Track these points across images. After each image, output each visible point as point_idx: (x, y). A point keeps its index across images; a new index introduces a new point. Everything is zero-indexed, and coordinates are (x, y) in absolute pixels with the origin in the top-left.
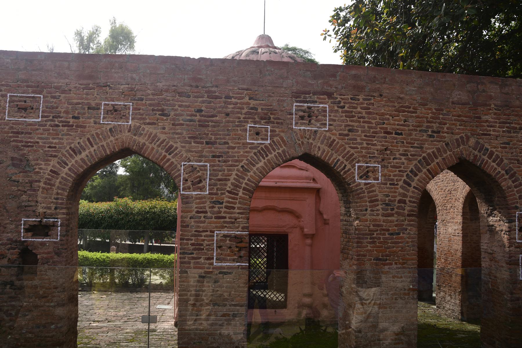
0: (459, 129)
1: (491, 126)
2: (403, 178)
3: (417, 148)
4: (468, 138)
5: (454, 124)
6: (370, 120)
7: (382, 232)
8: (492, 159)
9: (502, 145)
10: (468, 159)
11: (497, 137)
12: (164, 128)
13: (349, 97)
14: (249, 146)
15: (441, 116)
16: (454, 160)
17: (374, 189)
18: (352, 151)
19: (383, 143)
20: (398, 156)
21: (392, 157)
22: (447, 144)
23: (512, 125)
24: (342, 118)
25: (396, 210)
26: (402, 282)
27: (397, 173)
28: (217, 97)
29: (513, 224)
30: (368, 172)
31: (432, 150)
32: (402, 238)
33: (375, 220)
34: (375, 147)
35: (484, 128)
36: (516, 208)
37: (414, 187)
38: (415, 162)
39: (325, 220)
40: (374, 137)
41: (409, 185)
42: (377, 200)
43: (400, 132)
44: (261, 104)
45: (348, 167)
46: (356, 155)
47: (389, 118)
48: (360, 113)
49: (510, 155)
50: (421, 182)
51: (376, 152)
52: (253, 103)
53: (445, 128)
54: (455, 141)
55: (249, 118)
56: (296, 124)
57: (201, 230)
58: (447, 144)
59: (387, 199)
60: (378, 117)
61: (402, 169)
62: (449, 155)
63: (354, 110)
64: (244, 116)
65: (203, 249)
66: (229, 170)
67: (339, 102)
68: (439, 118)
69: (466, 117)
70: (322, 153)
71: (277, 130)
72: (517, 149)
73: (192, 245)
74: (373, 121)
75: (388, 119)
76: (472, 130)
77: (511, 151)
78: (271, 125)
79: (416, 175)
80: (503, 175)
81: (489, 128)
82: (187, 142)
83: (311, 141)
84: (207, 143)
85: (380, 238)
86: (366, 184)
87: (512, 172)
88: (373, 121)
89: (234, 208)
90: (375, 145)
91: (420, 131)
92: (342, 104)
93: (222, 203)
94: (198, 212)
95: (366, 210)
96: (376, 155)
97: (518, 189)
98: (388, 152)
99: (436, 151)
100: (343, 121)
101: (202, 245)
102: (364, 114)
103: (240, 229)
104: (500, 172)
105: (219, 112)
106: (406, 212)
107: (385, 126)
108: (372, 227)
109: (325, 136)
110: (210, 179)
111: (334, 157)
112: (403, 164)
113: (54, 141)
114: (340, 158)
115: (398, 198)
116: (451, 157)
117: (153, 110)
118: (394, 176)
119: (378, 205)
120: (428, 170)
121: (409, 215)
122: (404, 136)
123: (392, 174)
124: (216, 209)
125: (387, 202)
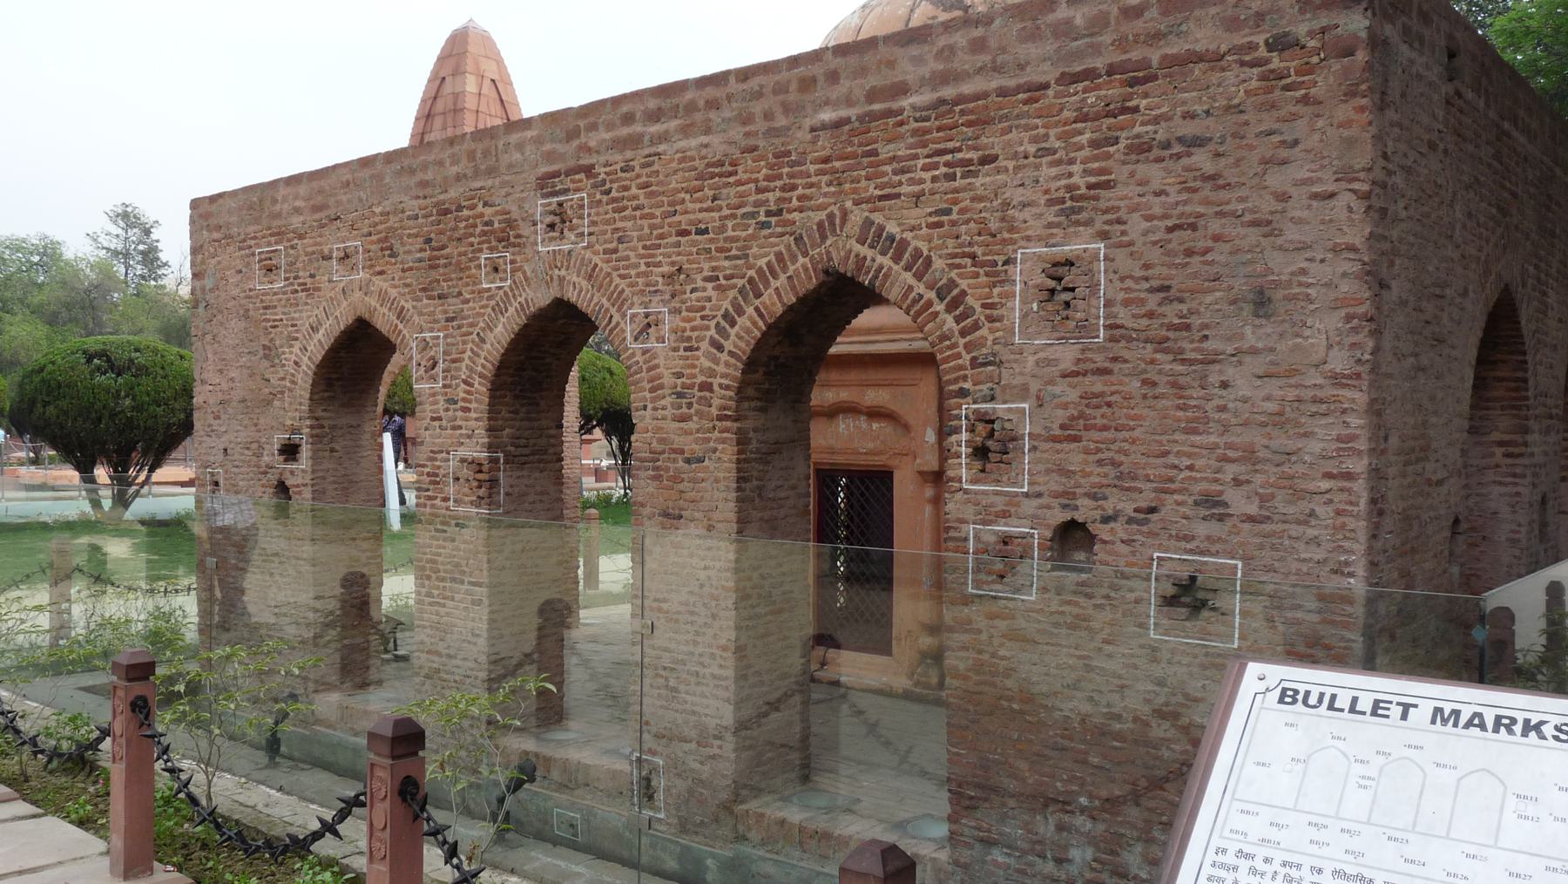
0: (825, 195)
1: (903, 171)
3: (737, 257)
4: (845, 214)
5: (811, 185)
6: (653, 210)
7: (673, 456)
8: (902, 263)
11: (918, 197)
12: (393, 279)
13: (618, 167)
14: (486, 295)
15: (786, 170)
16: (811, 278)
17: (656, 361)
18: (623, 284)
19: (674, 258)
20: (700, 284)
21: (688, 288)
23: (959, 156)
24: (608, 216)
26: (705, 568)
27: (698, 322)
28: (446, 212)
30: (649, 325)
31: (765, 260)
34: (660, 269)
35: (886, 179)
36: (963, 393)
37: (731, 353)
38: (732, 293)
40: (659, 246)
41: (720, 348)
42: (661, 387)
44: (497, 213)
45: (617, 318)
46: (628, 291)
47: (684, 199)
48: (635, 197)
49: (951, 242)
50: (740, 338)
51: (660, 279)
52: (488, 211)
53: (794, 199)
55: (483, 242)
57: (435, 449)
58: (799, 239)
59: (679, 381)
63: (626, 194)
64: (477, 240)
65: (438, 483)
66: (464, 343)
67: (604, 182)
68: (780, 177)
70: (579, 295)
71: (518, 259)
72: (972, 225)
73: (428, 474)
74: (658, 212)
75: (683, 201)
76: (855, 191)
78: (511, 249)
80: (930, 304)
81: (898, 178)
82: (418, 300)
84: (440, 298)
86: (645, 352)
87: (955, 292)
89: (469, 410)
90: (659, 264)
92: (608, 186)
94: (433, 419)
95: (645, 408)
96: (660, 287)
97: (968, 338)
98: (682, 277)
99: (774, 260)
100: (607, 222)
101: (437, 475)
102: (642, 200)
103: (478, 448)
104: (921, 296)
106: (714, 411)
107: (677, 218)
108: (655, 444)
109: (583, 259)
110: (444, 361)
111: (595, 300)
112: (709, 299)
113: (297, 315)
114: (604, 301)
115: (700, 379)
116: (806, 270)
117: (382, 249)
118: (693, 329)
119: (664, 397)
120: (757, 309)
121: (720, 418)
122: (711, 235)
123: (688, 325)
124: (450, 413)
125: (679, 389)
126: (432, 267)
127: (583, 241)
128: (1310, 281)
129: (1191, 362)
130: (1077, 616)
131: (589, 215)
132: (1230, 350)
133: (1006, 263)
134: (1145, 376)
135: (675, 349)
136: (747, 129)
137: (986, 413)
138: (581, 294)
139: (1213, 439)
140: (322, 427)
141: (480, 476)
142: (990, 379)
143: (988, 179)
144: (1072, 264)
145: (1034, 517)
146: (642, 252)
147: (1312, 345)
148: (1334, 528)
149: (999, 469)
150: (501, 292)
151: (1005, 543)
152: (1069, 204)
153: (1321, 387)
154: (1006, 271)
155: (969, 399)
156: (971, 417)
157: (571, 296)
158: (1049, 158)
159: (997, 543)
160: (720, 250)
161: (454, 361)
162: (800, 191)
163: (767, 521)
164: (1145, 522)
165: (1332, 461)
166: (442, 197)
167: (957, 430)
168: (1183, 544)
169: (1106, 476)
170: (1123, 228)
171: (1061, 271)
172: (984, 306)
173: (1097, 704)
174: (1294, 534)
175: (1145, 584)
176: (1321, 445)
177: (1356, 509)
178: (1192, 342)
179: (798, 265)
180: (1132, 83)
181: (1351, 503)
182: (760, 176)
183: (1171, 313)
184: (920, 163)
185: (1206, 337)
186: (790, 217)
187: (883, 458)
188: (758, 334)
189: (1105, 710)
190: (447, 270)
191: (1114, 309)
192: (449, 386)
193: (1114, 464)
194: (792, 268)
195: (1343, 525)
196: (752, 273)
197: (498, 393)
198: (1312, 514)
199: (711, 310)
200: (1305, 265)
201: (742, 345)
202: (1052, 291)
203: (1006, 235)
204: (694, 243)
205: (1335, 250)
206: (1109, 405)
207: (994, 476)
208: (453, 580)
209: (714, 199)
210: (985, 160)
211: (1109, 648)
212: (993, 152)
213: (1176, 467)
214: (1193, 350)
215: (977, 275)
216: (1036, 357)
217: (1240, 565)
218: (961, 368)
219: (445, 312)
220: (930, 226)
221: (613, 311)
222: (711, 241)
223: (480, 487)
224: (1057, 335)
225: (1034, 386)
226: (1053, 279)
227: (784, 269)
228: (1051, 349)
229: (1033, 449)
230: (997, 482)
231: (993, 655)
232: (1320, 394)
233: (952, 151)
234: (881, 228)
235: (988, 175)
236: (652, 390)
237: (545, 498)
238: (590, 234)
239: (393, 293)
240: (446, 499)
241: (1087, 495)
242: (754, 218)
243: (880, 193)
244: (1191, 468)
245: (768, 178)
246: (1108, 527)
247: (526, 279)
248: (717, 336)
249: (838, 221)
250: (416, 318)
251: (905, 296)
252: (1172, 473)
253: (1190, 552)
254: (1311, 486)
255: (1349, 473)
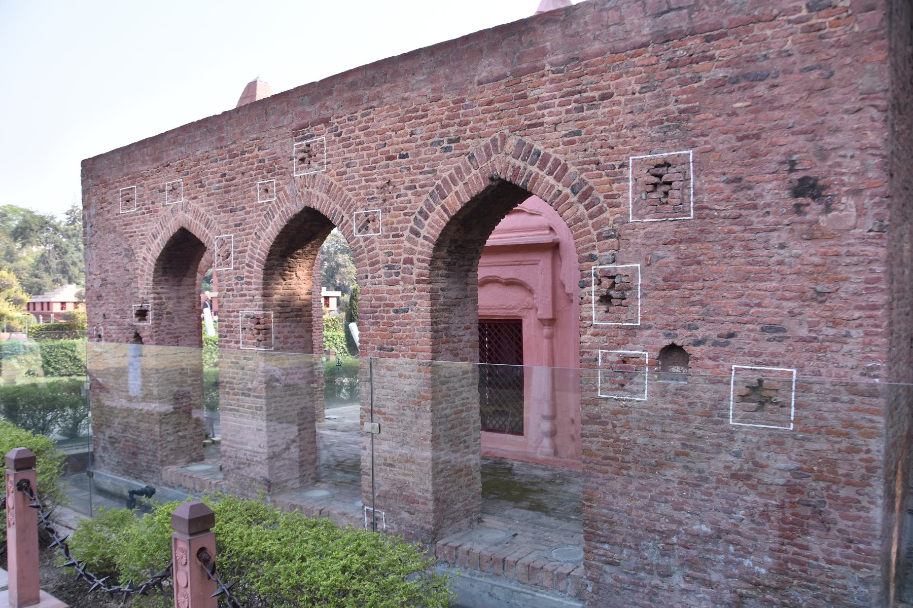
0: (490, 125)
1: (545, 108)
2: (409, 225)
3: (429, 173)
4: (504, 139)
5: (481, 120)
8: (546, 170)
9: (566, 139)
10: (503, 177)
13: (346, 118)
17: (373, 245)
18: (350, 194)
19: (385, 175)
20: (403, 191)
21: (395, 195)
22: (471, 157)
23: (585, 95)
25: (401, 274)
27: (402, 217)
28: (235, 156)
29: (586, 289)
30: (368, 221)
31: (449, 173)
32: (409, 317)
33: (377, 291)
35: (533, 113)
37: (425, 237)
38: (425, 197)
39: (568, 295)
40: (374, 168)
42: (377, 262)
43: (405, 153)
45: (346, 217)
46: (353, 199)
48: (357, 137)
49: (581, 154)
50: (432, 227)
51: (375, 190)
52: (261, 153)
54: (483, 149)
56: (297, 169)
58: (471, 157)
59: (390, 258)
60: (378, 136)
61: (408, 210)
62: (474, 175)
66: (247, 240)
68: (458, 116)
69: (500, 102)
72: (596, 141)
73: (226, 326)
74: (373, 145)
75: (391, 137)
76: (511, 123)
77: (584, 146)
78: (276, 177)
79: (426, 217)
83: (310, 190)
85: (383, 318)
86: (366, 239)
87: (585, 188)
88: (373, 145)
89: (250, 283)
90: (374, 180)
91: (432, 144)
93: (242, 279)
94: (228, 290)
95: (367, 277)
96: (376, 195)
98: (391, 187)
100: (339, 155)
102: (363, 138)
104: (560, 192)
105: (237, 173)
106: (414, 277)
107: (387, 148)
108: (374, 302)
111: (332, 206)
114: (338, 207)
115: (404, 256)
116: (477, 178)
117: (195, 183)
118: (399, 222)
120: (443, 207)
121: (418, 282)
122: (410, 158)
123: (395, 220)
124: (239, 286)
126: (226, 192)
127: (323, 168)
128: (843, 170)
129: (758, 231)
130: (676, 411)
131: (327, 151)
132: (786, 222)
133: (621, 166)
134: (725, 242)
135: (387, 237)
136: (434, 86)
137: (609, 271)
138: (321, 203)
139: (774, 284)
140: (161, 298)
141: (258, 326)
142: (611, 247)
143: (606, 110)
144: (669, 165)
145: (645, 343)
146: (363, 172)
147: (846, 216)
148: (864, 343)
149: (619, 310)
150: (270, 205)
151: (624, 362)
152: (666, 124)
153: (852, 245)
154: (621, 172)
155: (597, 262)
156: (598, 273)
157: (316, 205)
158: (650, 93)
159: (618, 362)
160: (416, 168)
161: (240, 252)
162: (472, 125)
163: (451, 351)
164: (728, 344)
165: (861, 298)
166: (232, 147)
167: (588, 284)
168: (754, 359)
169: (697, 312)
170: (706, 139)
171: (660, 171)
172: (606, 197)
173: (691, 470)
174: (834, 348)
175: (725, 387)
176: (854, 286)
177: (880, 330)
178: (758, 217)
179: (472, 174)
180: (708, 40)
181: (876, 326)
182: (444, 117)
183: (742, 197)
184: (557, 101)
185: (768, 213)
186: (465, 142)
187: (516, 311)
188: (445, 224)
189: (696, 475)
190: (235, 193)
191: (700, 196)
192: (238, 269)
193: (702, 304)
194: (467, 177)
195: (871, 341)
196: (439, 182)
197: (269, 272)
198: (848, 335)
199: (411, 209)
200: (839, 160)
201: (432, 231)
202: (655, 185)
203: (621, 147)
204: (399, 165)
205: (863, 149)
206: (699, 263)
207: (614, 316)
208: (243, 394)
209: (412, 134)
210: (603, 98)
211: (700, 433)
212: (610, 91)
213: (748, 305)
214: (759, 223)
215: (601, 176)
216: (645, 231)
217: (795, 371)
218: (591, 240)
219: (235, 220)
220: (565, 144)
221: (344, 213)
222: (410, 162)
223: (259, 334)
224: (658, 215)
225: (644, 251)
226: (655, 175)
227: (462, 178)
228: (656, 225)
229: (644, 295)
230: (618, 319)
231: (617, 440)
232: (852, 249)
233: (580, 92)
234: (531, 147)
235: (605, 107)
236: (372, 264)
237: (300, 340)
238: (328, 163)
239: (202, 210)
240: (237, 342)
241: (683, 327)
242: (439, 145)
243: (527, 122)
244: (759, 305)
245: (449, 118)
246: (698, 348)
247: (286, 195)
248: (415, 227)
249: (499, 143)
250: (217, 226)
251: (549, 192)
252: (745, 309)
253: (759, 364)
254: (845, 316)
255: (874, 305)
